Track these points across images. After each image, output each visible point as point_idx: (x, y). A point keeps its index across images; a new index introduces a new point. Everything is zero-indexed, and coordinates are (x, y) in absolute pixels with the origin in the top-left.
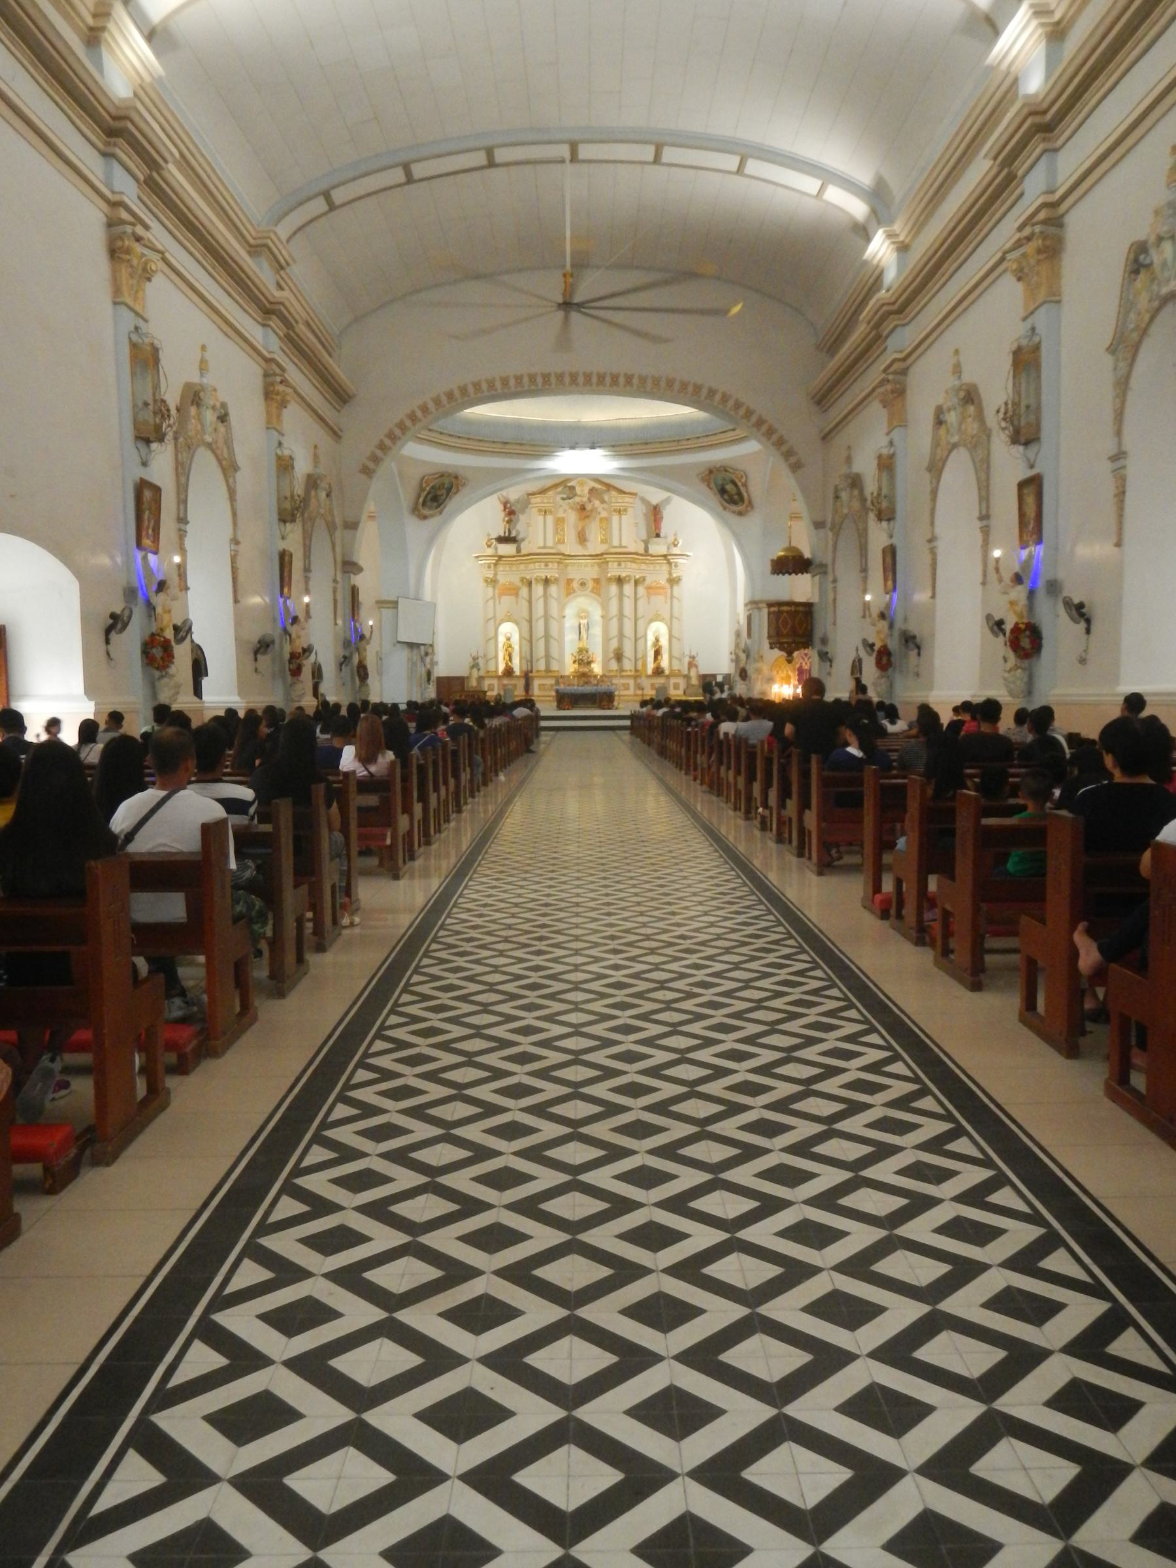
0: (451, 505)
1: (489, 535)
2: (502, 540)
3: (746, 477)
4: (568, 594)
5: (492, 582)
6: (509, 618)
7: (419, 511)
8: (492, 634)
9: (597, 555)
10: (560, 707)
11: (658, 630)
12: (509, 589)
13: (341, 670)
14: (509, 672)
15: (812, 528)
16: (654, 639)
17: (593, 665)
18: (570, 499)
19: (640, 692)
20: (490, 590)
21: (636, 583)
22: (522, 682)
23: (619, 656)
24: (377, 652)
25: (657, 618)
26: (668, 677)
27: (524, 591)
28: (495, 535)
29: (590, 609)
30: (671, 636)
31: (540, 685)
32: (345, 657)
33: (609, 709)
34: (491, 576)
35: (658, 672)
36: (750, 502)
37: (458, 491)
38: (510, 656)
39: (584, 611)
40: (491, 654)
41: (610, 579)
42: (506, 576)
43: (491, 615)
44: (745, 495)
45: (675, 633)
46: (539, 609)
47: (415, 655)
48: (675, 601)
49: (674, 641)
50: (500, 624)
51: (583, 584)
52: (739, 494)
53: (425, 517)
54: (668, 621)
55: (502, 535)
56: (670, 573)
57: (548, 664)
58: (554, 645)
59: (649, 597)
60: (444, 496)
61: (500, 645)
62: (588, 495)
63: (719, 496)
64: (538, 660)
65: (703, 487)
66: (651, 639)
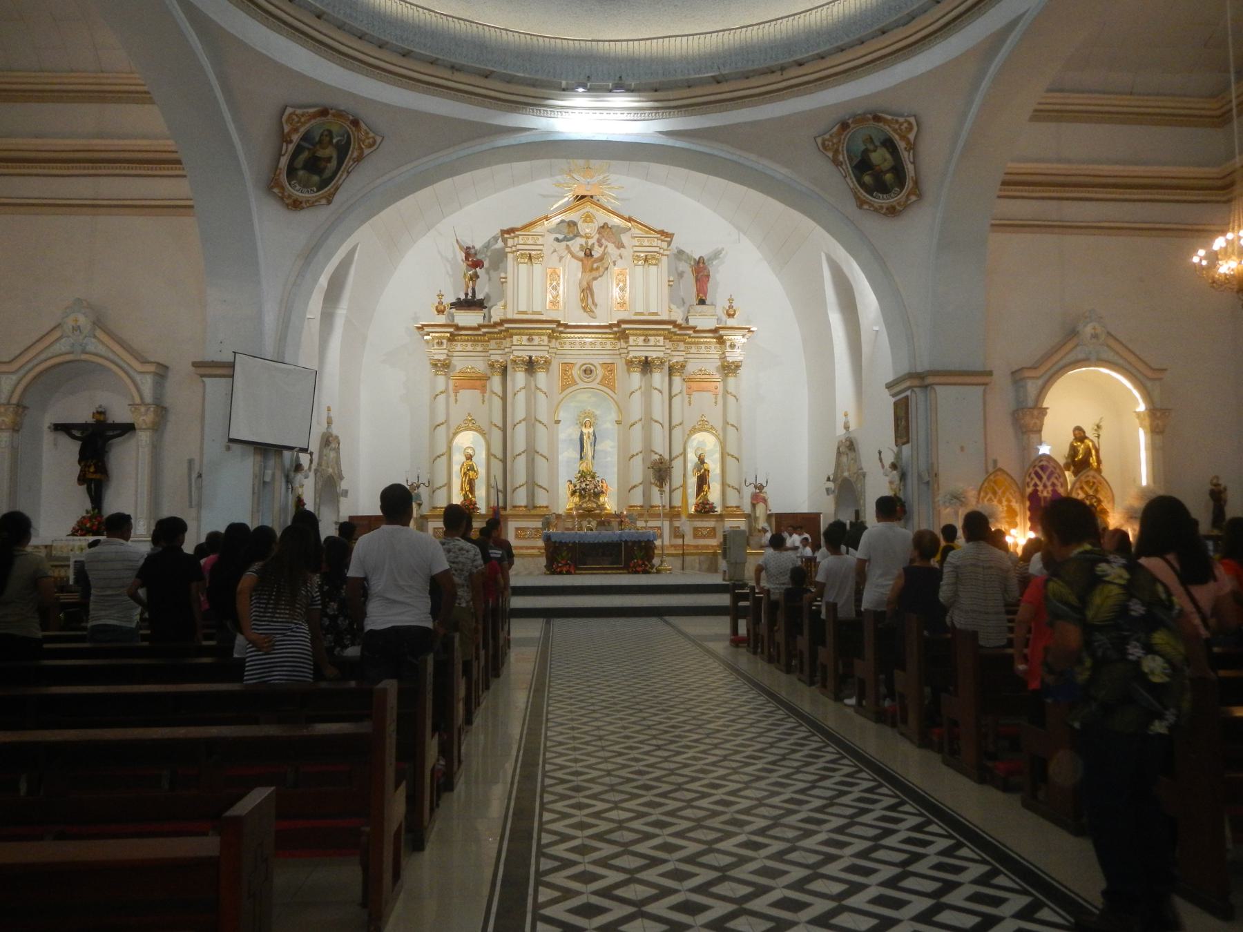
0: (352, 184)
1: (440, 296)
2: (461, 304)
4: (564, 388)
5: (443, 367)
6: (470, 424)
7: (282, 188)
8: (442, 448)
9: (611, 326)
10: (552, 569)
11: (706, 442)
12: (471, 379)
17: (602, 499)
18: (571, 239)
19: (680, 541)
20: (441, 381)
21: (671, 369)
23: (661, 472)
24: (190, 462)
25: (703, 426)
26: (721, 517)
27: (496, 380)
28: (450, 299)
29: (597, 412)
30: (724, 455)
31: (517, 529)
33: (646, 572)
34: (442, 357)
35: (705, 509)
36: (916, 183)
37: (359, 159)
38: (471, 483)
39: (587, 414)
40: (441, 480)
41: (630, 363)
42: (468, 359)
43: (441, 419)
44: (910, 168)
45: (732, 449)
46: (519, 409)
47: (272, 470)
48: (731, 399)
49: (729, 459)
50: (455, 434)
51: (588, 372)
52: (898, 171)
53: (296, 205)
54: (720, 432)
55: (463, 297)
56: (723, 358)
57: (531, 495)
58: (541, 463)
60: (333, 164)
61: (456, 468)
62: (597, 236)
63: (852, 182)
64: (514, 490)
65: (823, 166)
66: (692, 458)
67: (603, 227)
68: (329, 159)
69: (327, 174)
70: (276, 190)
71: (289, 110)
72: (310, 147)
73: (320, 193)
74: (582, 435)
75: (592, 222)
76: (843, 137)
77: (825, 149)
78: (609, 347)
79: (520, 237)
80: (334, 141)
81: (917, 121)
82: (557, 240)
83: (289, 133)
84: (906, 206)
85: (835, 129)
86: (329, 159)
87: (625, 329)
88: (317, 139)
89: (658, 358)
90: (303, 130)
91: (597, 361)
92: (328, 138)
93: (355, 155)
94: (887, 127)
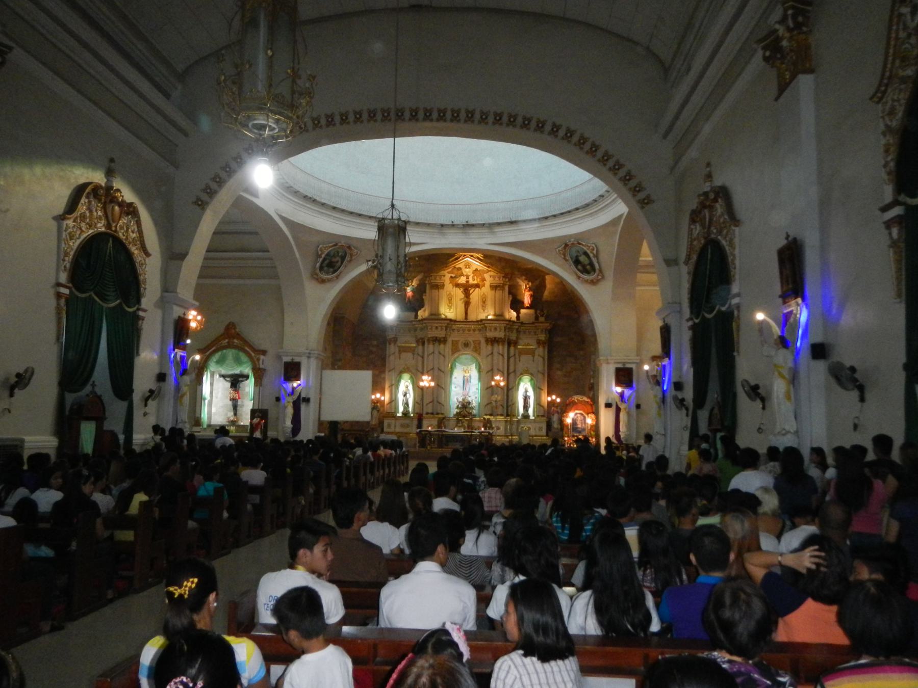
3: (597, 248)
7: (317, 275)
13: (146, 405)
14: (406, 414)
15: (664, 265)
16: (524, 391)
21: (509, 345)
22: (415, 422)
32: (151, 392)
36: (600, 271)
37: (350, 261)
52: (591, 264)
53: (323, 281)
59: (520, 356)
62: (472, 275)
63: (573, 267)
67: (475, 270)
68: (337, 262)
69: (336, 268)
70: (315, 276)
71: (321, 246)
72: (330, 258)
73: (334, 275)
74: (464, 377)
75: (469, 268)
76: (567, 249)
77: (560, 253)
78: (477, 332)
79: (433, 277)
80: (340, 254)
81: (597, 248)
82: (451, 277)
83: (321, 254)
84: (598, 281)
85: (563, 246)
86: (337, 262)
87: (484, 324)
88: (332, 255)
89: (501, 338)
90: (326, 252)
91: (471, 340)
92: (336, 254)
93: (349, 259)
94: (584, 247)
